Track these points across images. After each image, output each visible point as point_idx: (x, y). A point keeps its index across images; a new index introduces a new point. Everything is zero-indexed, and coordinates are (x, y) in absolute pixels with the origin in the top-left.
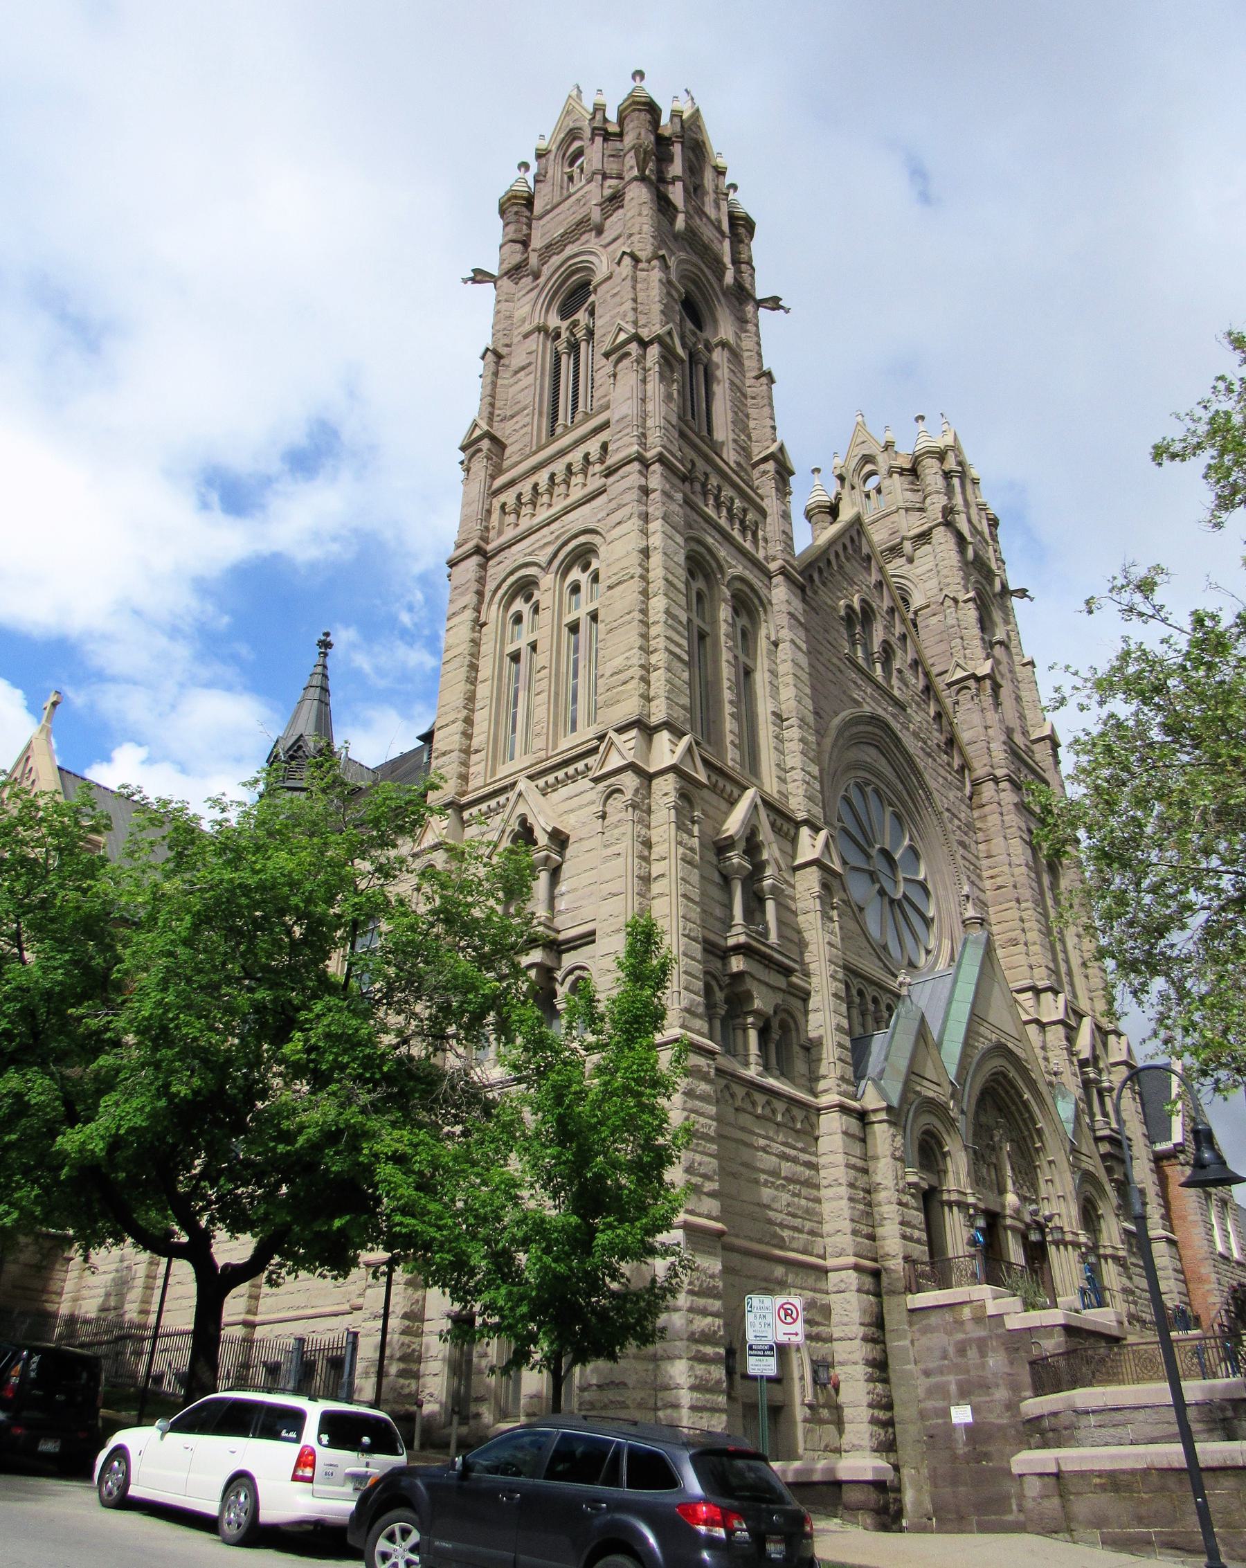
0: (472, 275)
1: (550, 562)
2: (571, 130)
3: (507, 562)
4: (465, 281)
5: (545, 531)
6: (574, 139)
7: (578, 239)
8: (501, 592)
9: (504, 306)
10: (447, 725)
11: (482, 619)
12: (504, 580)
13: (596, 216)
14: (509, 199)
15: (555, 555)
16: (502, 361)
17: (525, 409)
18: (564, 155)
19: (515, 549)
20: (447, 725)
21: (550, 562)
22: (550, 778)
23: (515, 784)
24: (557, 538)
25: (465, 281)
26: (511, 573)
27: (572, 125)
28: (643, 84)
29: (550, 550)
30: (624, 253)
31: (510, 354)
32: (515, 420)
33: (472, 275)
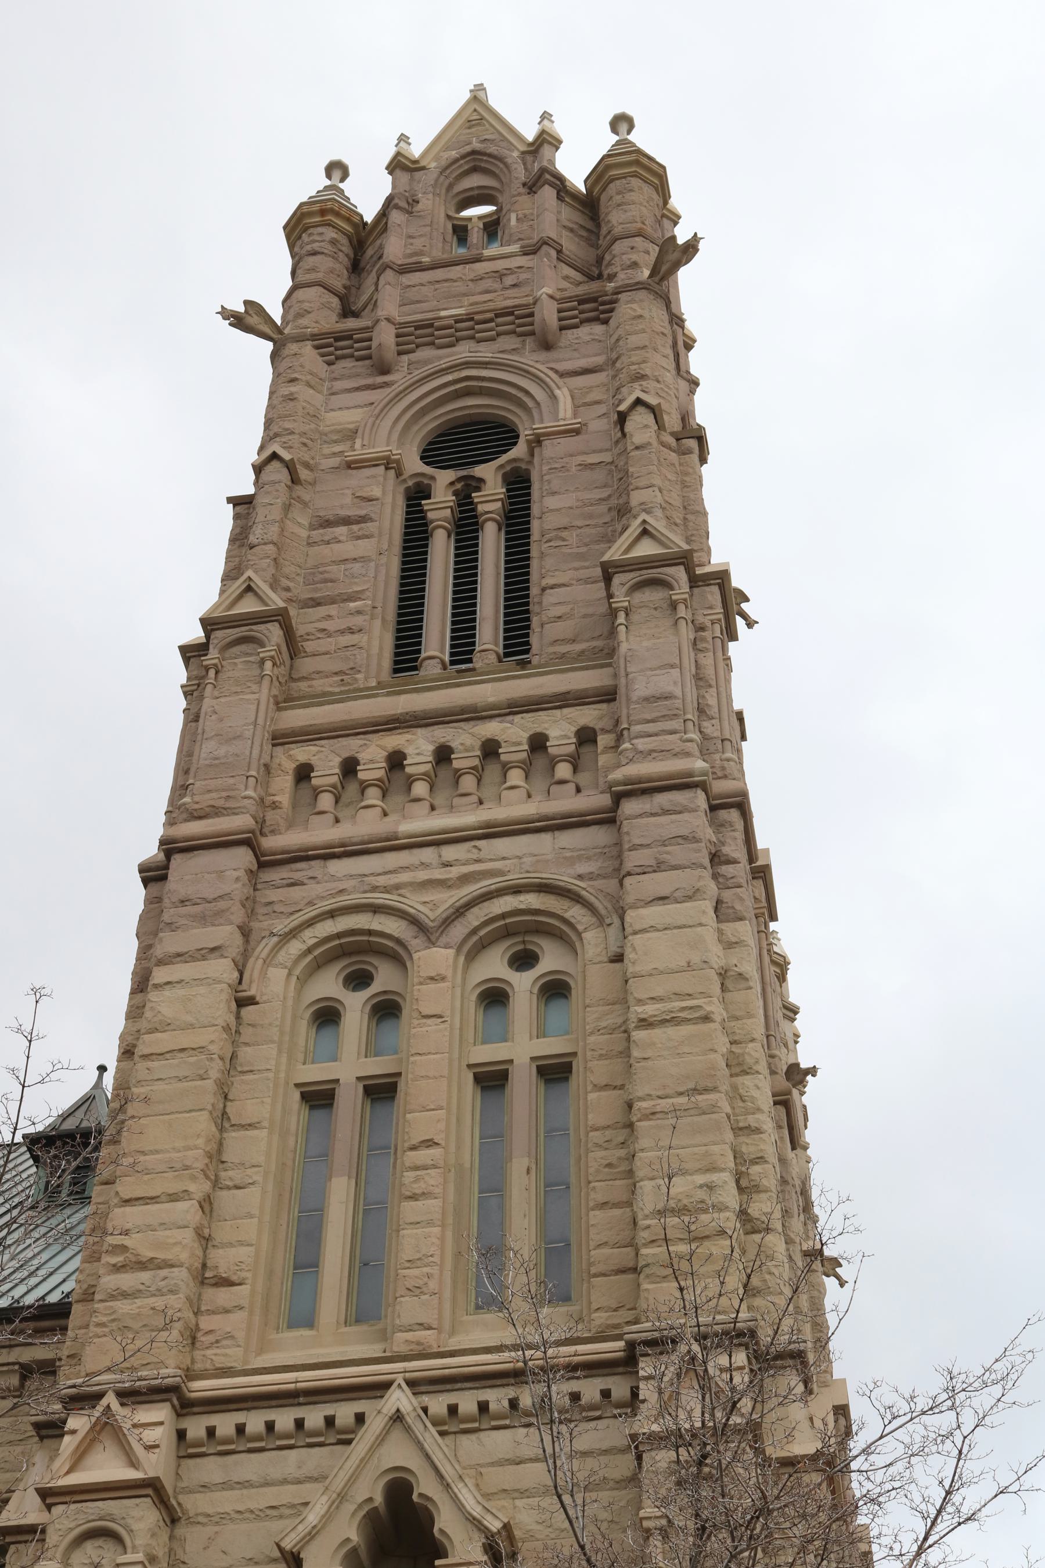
0: (241, 309)
1: (447, 922)
2: (473, 152)
3: (313, 890)
4: (226, 314)
5: (427, 854)
7: (492, 339)
9: (286, 390)
10: (153, 1199)
12: (310, 923)
13: (548, 314)
14: (323, 212)
15: (460, 911)
16: (299, 490)
17: (351, 598)
18: (450, 187)
19: (336, 867)
20: (153, 1199)
21: (447, 922)
22: (467, 1402)
23: (386, 1386)
24: (465, 879)
26: (332, 914)
27: (476, 145)
28: (630, 137)
29: (448, 899)
30: (638, 402)
31: (313, 484)
32: (322, 611)
33: (241, 309)
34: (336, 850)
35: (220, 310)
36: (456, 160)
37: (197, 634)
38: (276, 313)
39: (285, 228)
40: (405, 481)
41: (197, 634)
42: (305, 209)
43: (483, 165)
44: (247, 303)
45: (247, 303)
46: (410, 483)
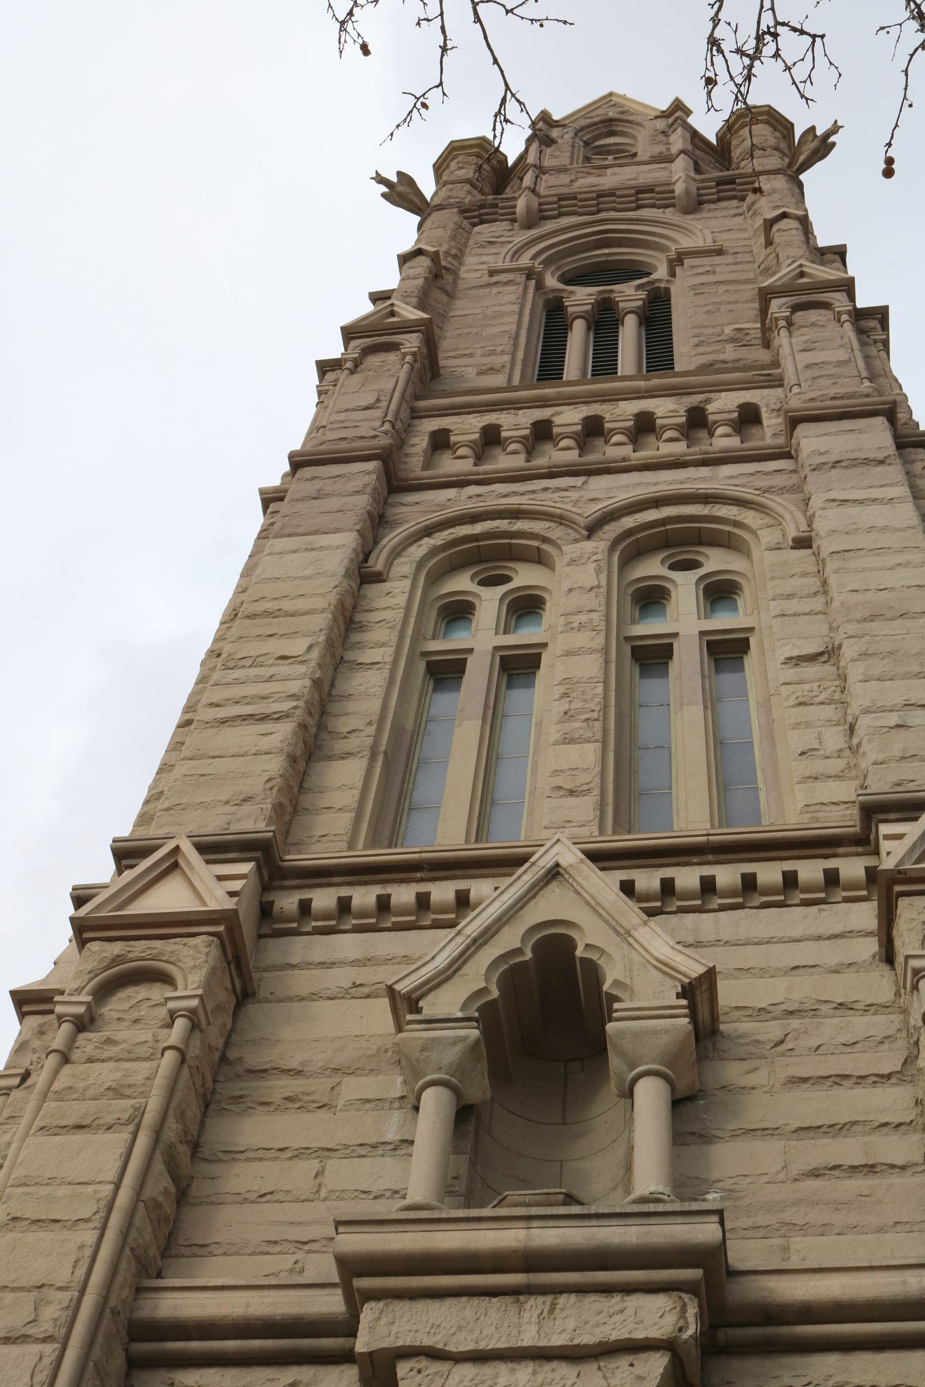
0: (394, 179)
4: (380, 179)
6: (612, 134)
8: (428, 543)
11: (378, 563)
25: (380, 179)
33: (394, 179)
34: (472, 477)
35: (374, 175)
36: (595, 124)
37: (335, 349)
38: (427, 187)
39: (434, 166)
40: (546, 293)
41: (335, 349)
42: (455, 145)
43: (619, 129)
44: (400, 174)
45: (400, 174)
46: (551, 296)
